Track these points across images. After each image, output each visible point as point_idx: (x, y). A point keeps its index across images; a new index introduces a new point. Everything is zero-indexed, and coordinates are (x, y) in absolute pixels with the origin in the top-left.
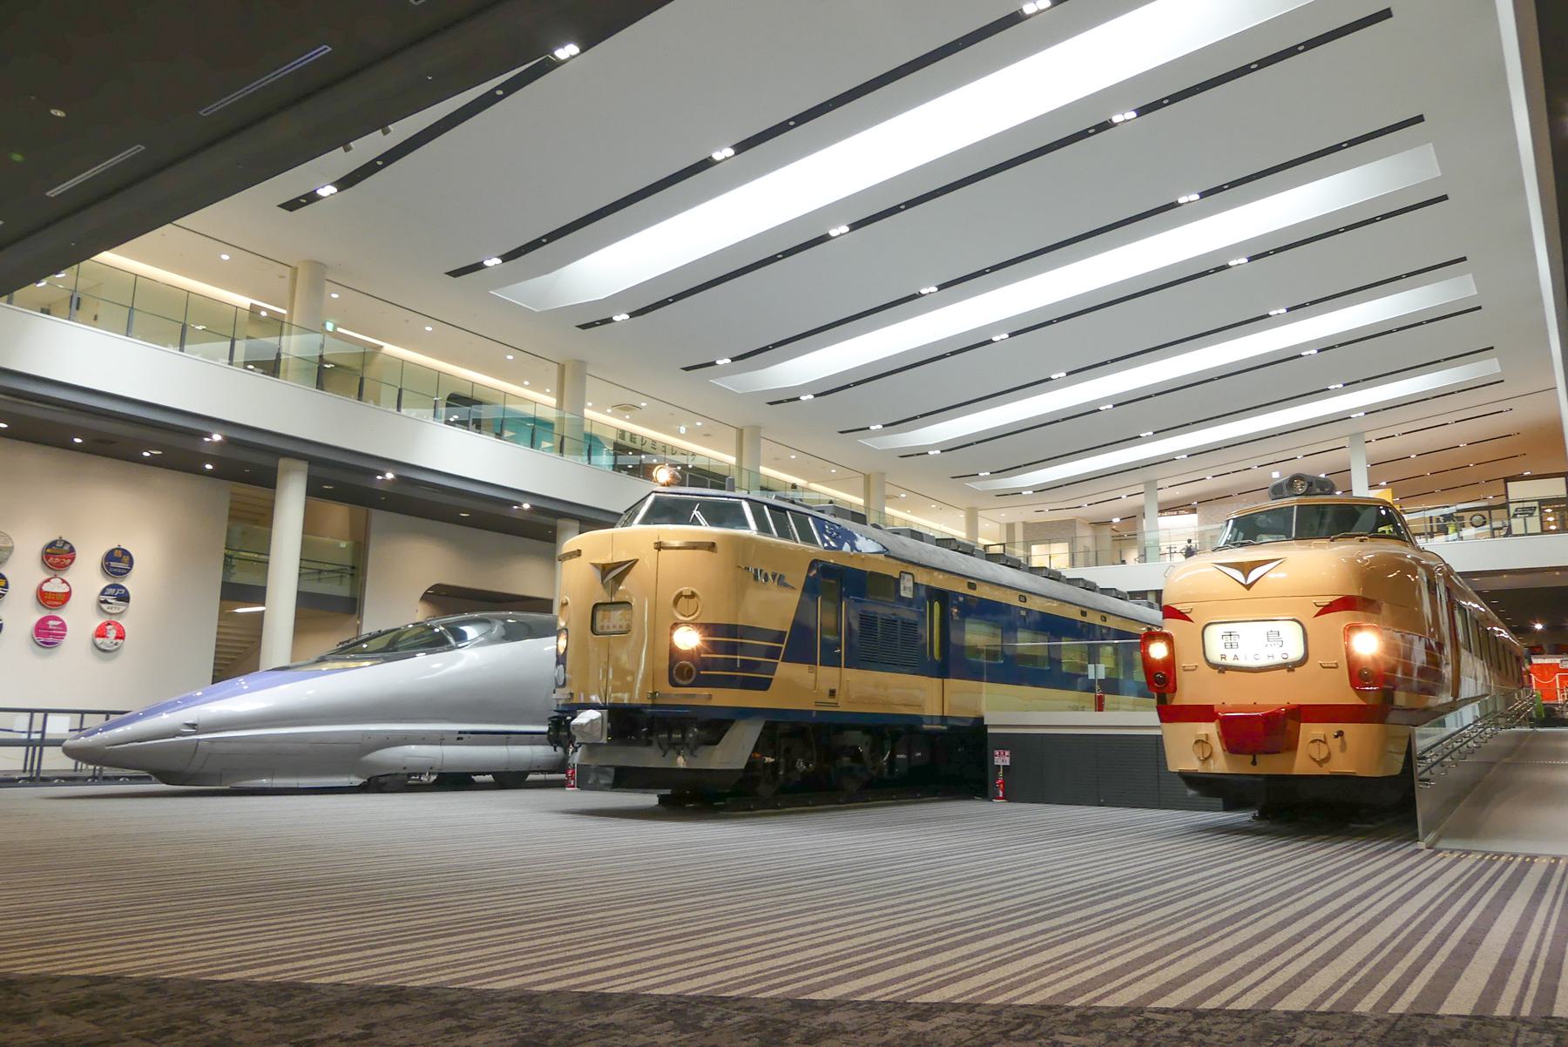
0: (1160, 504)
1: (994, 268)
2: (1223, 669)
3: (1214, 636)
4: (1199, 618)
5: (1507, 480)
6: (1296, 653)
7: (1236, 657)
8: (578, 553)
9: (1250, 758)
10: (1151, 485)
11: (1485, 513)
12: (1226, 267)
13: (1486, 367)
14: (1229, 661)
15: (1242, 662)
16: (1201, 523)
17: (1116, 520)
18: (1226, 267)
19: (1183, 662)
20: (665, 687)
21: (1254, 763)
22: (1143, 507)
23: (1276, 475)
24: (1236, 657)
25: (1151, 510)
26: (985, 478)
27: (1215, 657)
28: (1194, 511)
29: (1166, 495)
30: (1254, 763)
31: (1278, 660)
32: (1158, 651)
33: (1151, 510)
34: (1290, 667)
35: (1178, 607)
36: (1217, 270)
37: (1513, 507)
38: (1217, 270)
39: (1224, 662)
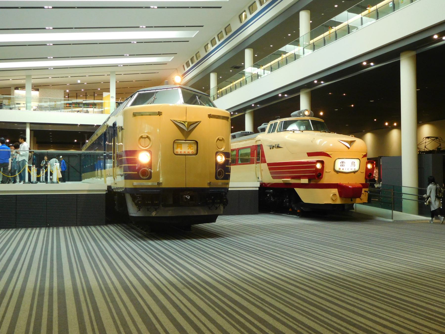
0: (33, 84)
2: (338, 172)
3: (338, 162)
4: (334, 157)
7: (343, 169)
8: (160, 114)
9: (350, 199)
12: (149, 8)
13: (169, 59)
14: (341, 170)
15: (344, 171)
16: (40, 94)
18: (149, 8)
19: (326, 169)
20: (214, 180)
21: (352, 200)
22: (25, 84)
23: (79, 82)
24: (343, 169)
25: (29, 87)
27: (337, 168)
28: (38, 90)
29: (34, 81)
30: (352, 200)
31: (353, 170)
32: (319, 166)
33: (29, 87)
34: (355, 172)
35: (328, 153)
39: (340, 170)
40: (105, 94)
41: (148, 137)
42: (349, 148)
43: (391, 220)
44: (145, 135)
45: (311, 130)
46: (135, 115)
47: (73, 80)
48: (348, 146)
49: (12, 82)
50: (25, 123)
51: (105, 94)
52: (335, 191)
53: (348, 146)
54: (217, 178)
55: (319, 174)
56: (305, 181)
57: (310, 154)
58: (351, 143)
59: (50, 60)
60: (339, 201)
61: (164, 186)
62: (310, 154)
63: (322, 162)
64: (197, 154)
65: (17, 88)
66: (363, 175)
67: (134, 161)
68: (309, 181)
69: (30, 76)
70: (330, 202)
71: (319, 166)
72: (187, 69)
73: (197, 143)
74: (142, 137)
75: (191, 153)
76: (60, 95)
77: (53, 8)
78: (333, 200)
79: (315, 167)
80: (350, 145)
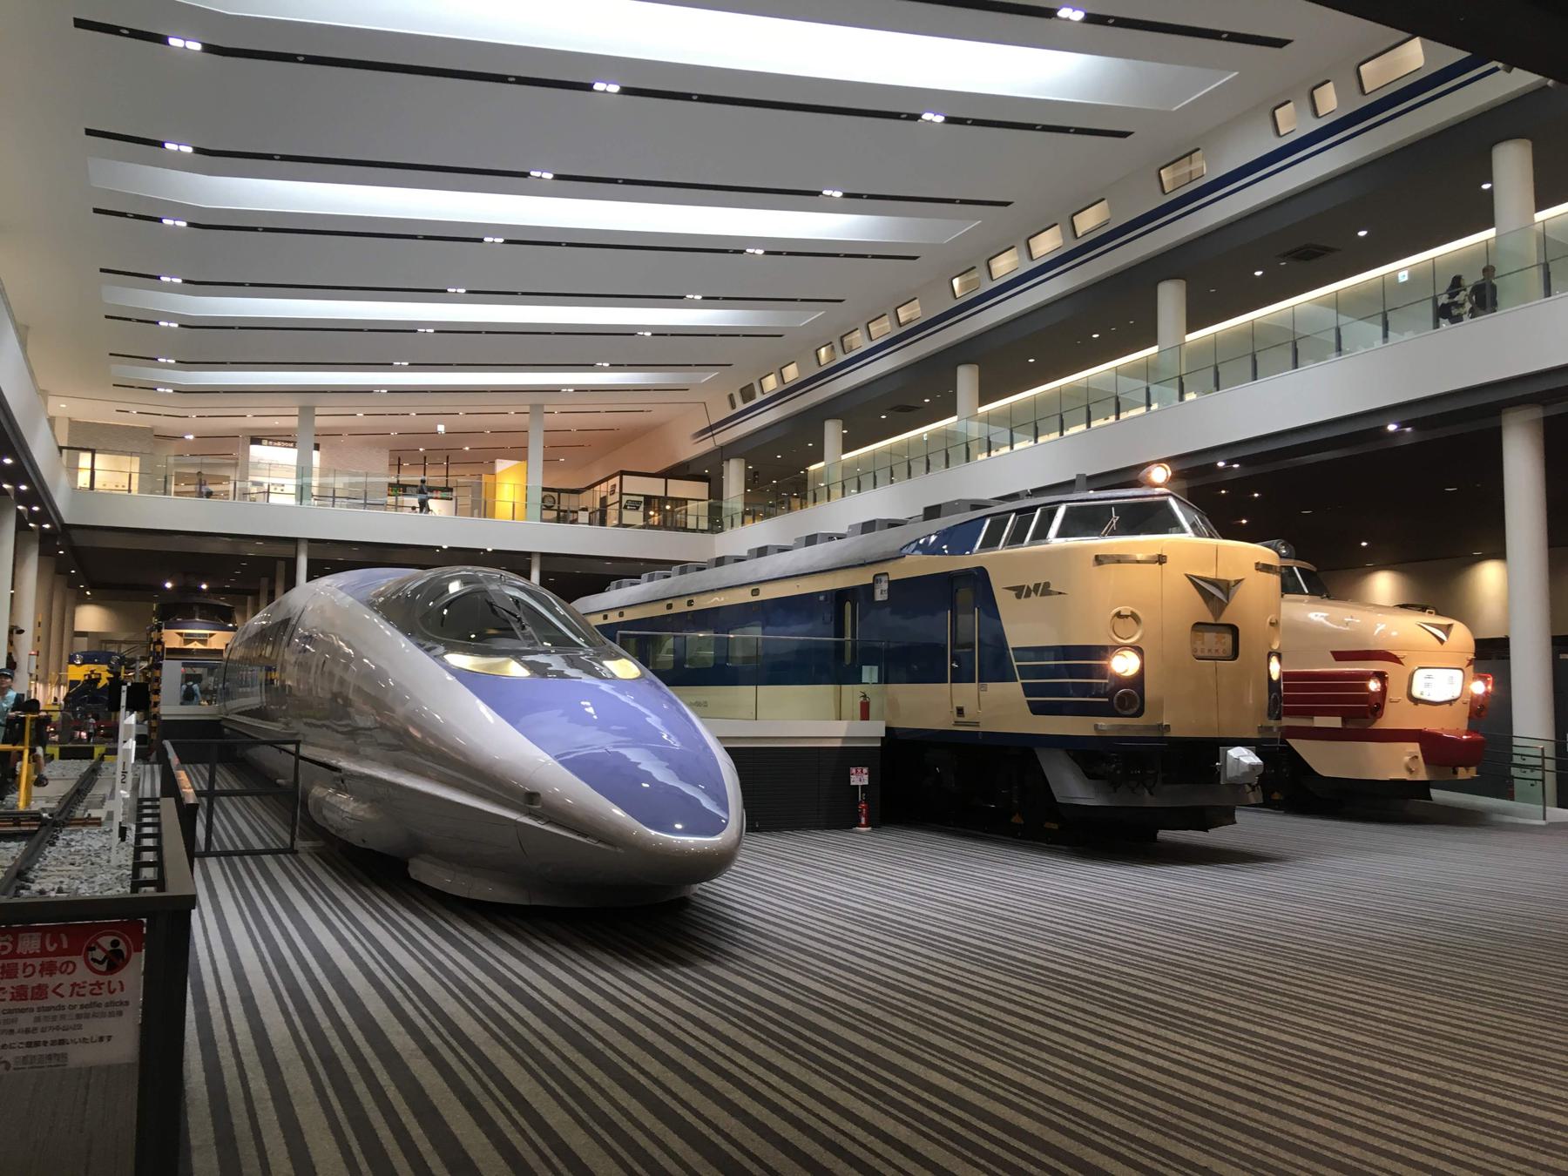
1: (627, 182)
2: (1416, 701)
3: (1419, 677)
4: (1410, 664)
5: (622, 473)
6: (1457, 694)
8: (1161, 560)
10: (307, 412)
11: (555, 495)
17: (191, 437)
19: (1390, 695)
21: (1455, 773)
26: (167, 366)
27: (1416, 693)
28: (317, 447)
31: (1448, 697)
32: (1374, 686)
34: (1450, 702)
36: (736, 252)
37: (625, 498)
38: (736, 252)
40: (502, 465)
41: (1134, 616)
42: (1442, 641)
43: (1542, 823)
44: (1125, 610)
45: (1302, 592)
46: (1099, 560)
47: (413, 421)
48: (1443, 636)
49: (252, 422)
50: (295, 541)
51: (502, 465)
52: (1414, 748)
53: (1443, 636)
54: (1270, 715)
55: (1376, 705)
56: (1335, 722)
57: (1339, 656)
58: (1447, 629)
59: (401, 369)
60: (1422, 775)
61: (1173, 734)
62: (1339, 656)
63: (1381, 676)
64: (1235, 654)
65: (256, 441)
66: (1467, 708)
67: (1103, 672)
68: (1344, 721)
69: (313, 408)
70: (1405, 776)
71: (1374, 686)
72: (741, 406)
73: (1234, 630)
74: (1118, 615)
75: (1221, 654)
76: (382, 461)
77: (507, 242)
78: (1410, 771)
79: (1365, 688)
80: (1447, 635)
